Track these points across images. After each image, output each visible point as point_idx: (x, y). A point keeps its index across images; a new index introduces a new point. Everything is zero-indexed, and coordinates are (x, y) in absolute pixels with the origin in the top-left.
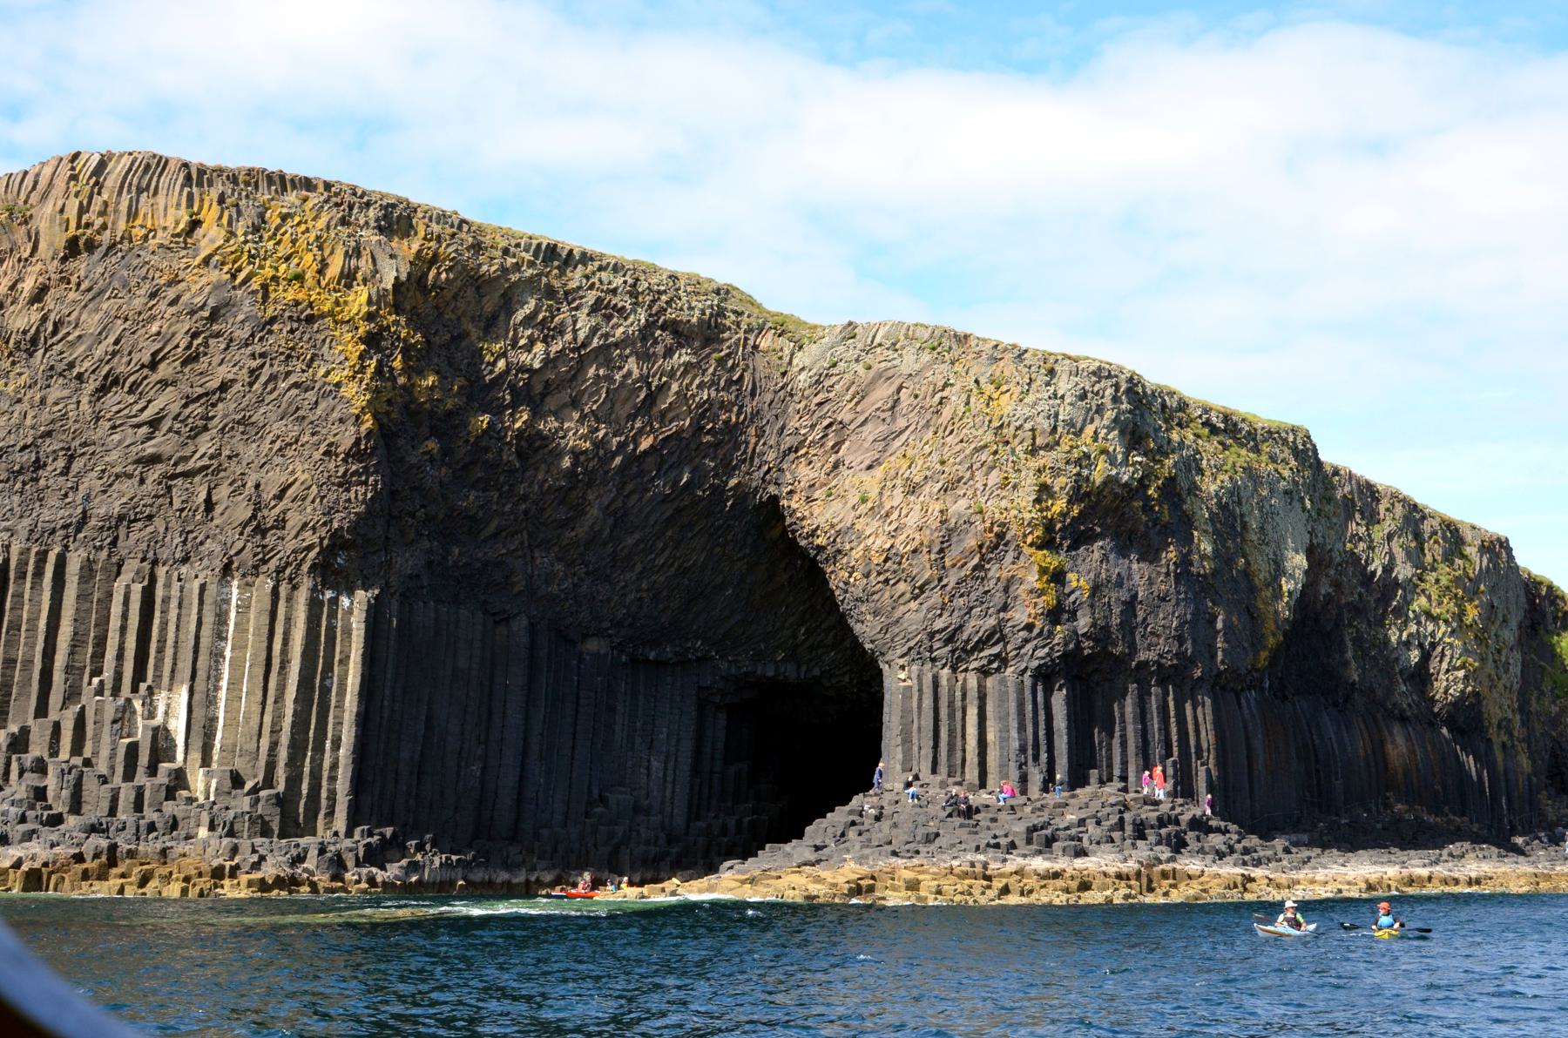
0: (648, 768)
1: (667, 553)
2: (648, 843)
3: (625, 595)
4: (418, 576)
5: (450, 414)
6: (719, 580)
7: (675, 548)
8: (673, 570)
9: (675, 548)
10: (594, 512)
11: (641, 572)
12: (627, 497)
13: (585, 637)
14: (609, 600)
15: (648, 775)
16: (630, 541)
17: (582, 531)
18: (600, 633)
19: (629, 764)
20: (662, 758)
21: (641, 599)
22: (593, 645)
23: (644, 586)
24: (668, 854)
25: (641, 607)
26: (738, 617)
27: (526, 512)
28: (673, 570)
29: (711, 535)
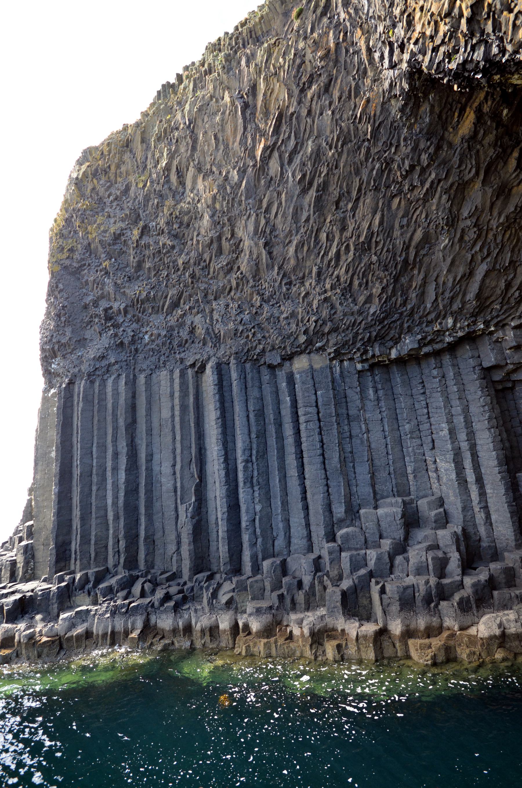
0: (436, 470)
1: (335, 243)
2: (420, 571)
3: (310, 304)
4: (103, 357)
5: (117, 237)
6: (419, 235)
7: (343, 229)
8: (351, 253)
9: (343, 229)
10: (247, 243)
11: (319, 274)
12: (268, 210)
13: (290, 358)
14: (293, 315)
15: (439, 478)
16: (292, 250)
17: (244, 264)
18: (307, 348)
19: (409, 470)
20: (450, 456)
21: (326, 300)
22: (300, 364)
23: (328, 286)
24: (461, 585)
25: (332, 307)
26: (482, 270)
27: (193, 276)
28: (351, 253)
29: (377, 189)
